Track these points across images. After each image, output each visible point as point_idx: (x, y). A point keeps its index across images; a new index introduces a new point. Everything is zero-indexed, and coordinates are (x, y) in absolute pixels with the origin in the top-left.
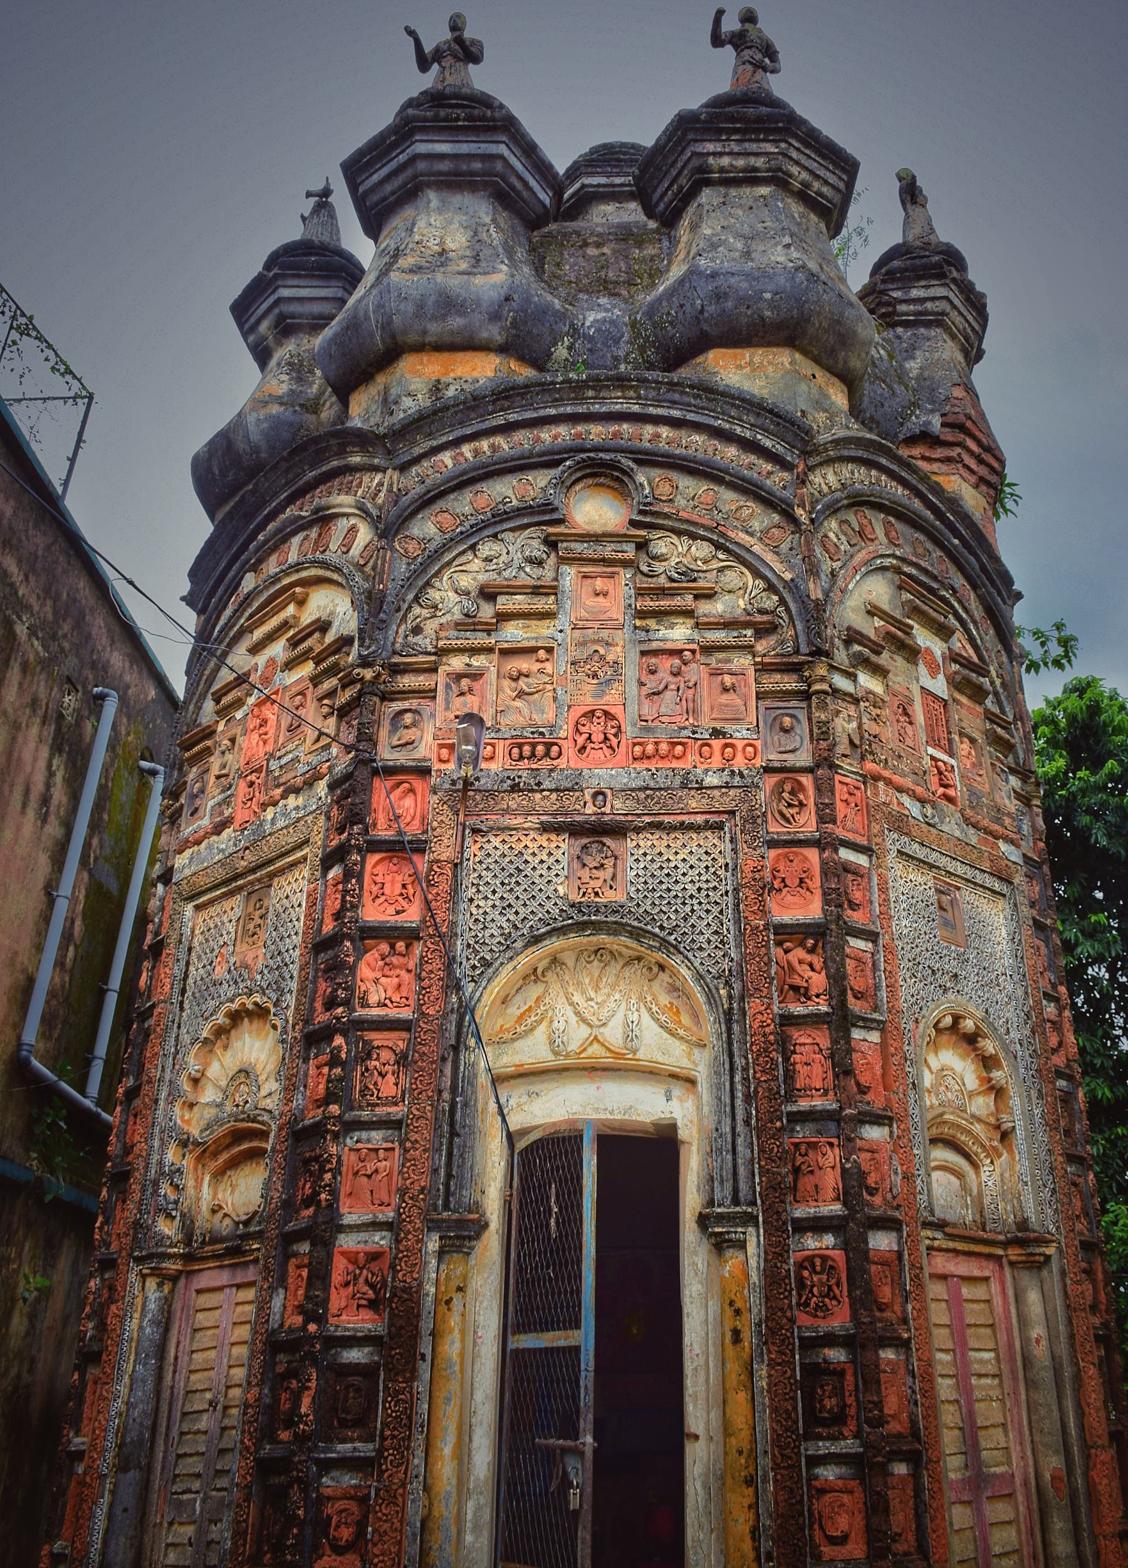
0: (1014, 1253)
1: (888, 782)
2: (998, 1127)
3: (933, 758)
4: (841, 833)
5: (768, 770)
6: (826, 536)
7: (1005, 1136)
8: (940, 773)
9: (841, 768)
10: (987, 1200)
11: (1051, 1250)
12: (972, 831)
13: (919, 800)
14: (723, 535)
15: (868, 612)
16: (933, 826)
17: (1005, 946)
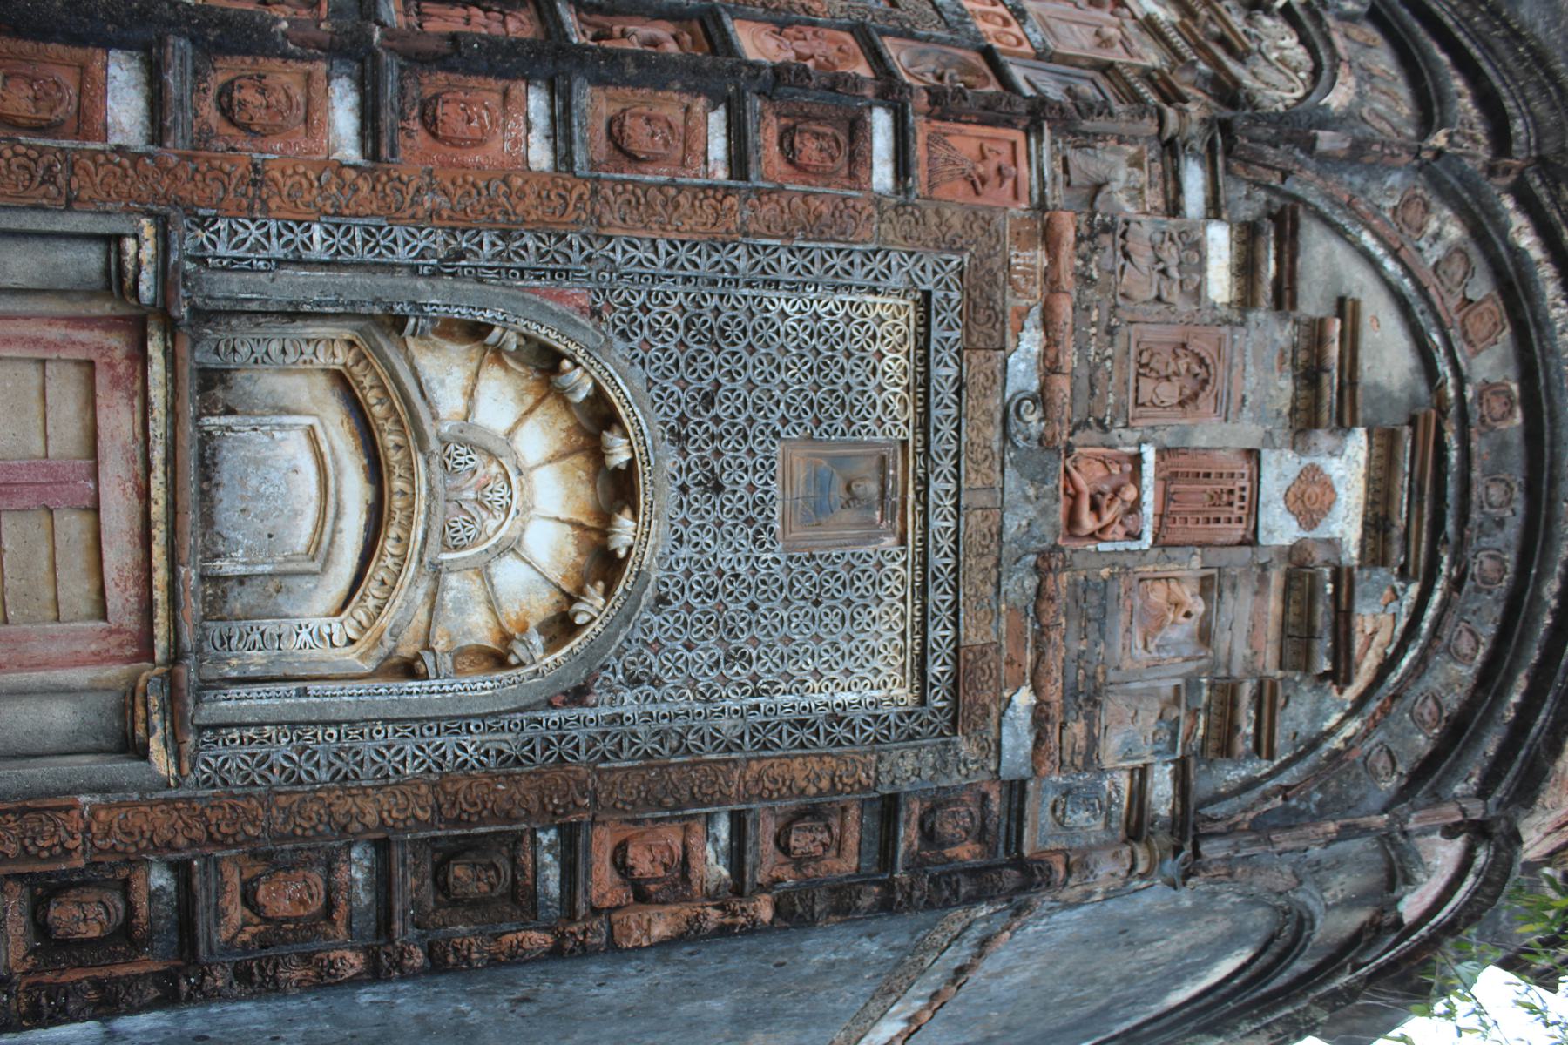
0: (150, 673)
1: (1052, 285)
2: (427, 646)
3: (1137, 459)
4: (921, 128)
5: (988, 54)
6: (1427, 208)
7: (409, 669)
8: (1116, 492)
9: (1040, 141)
10: (269, 625)
11: (161, 761)
12: (1031, 583)
13: (1044, 387)
14: (1335, 67)
15: (1341, 301)
16: (1006, 436)
17: (819, 697)
